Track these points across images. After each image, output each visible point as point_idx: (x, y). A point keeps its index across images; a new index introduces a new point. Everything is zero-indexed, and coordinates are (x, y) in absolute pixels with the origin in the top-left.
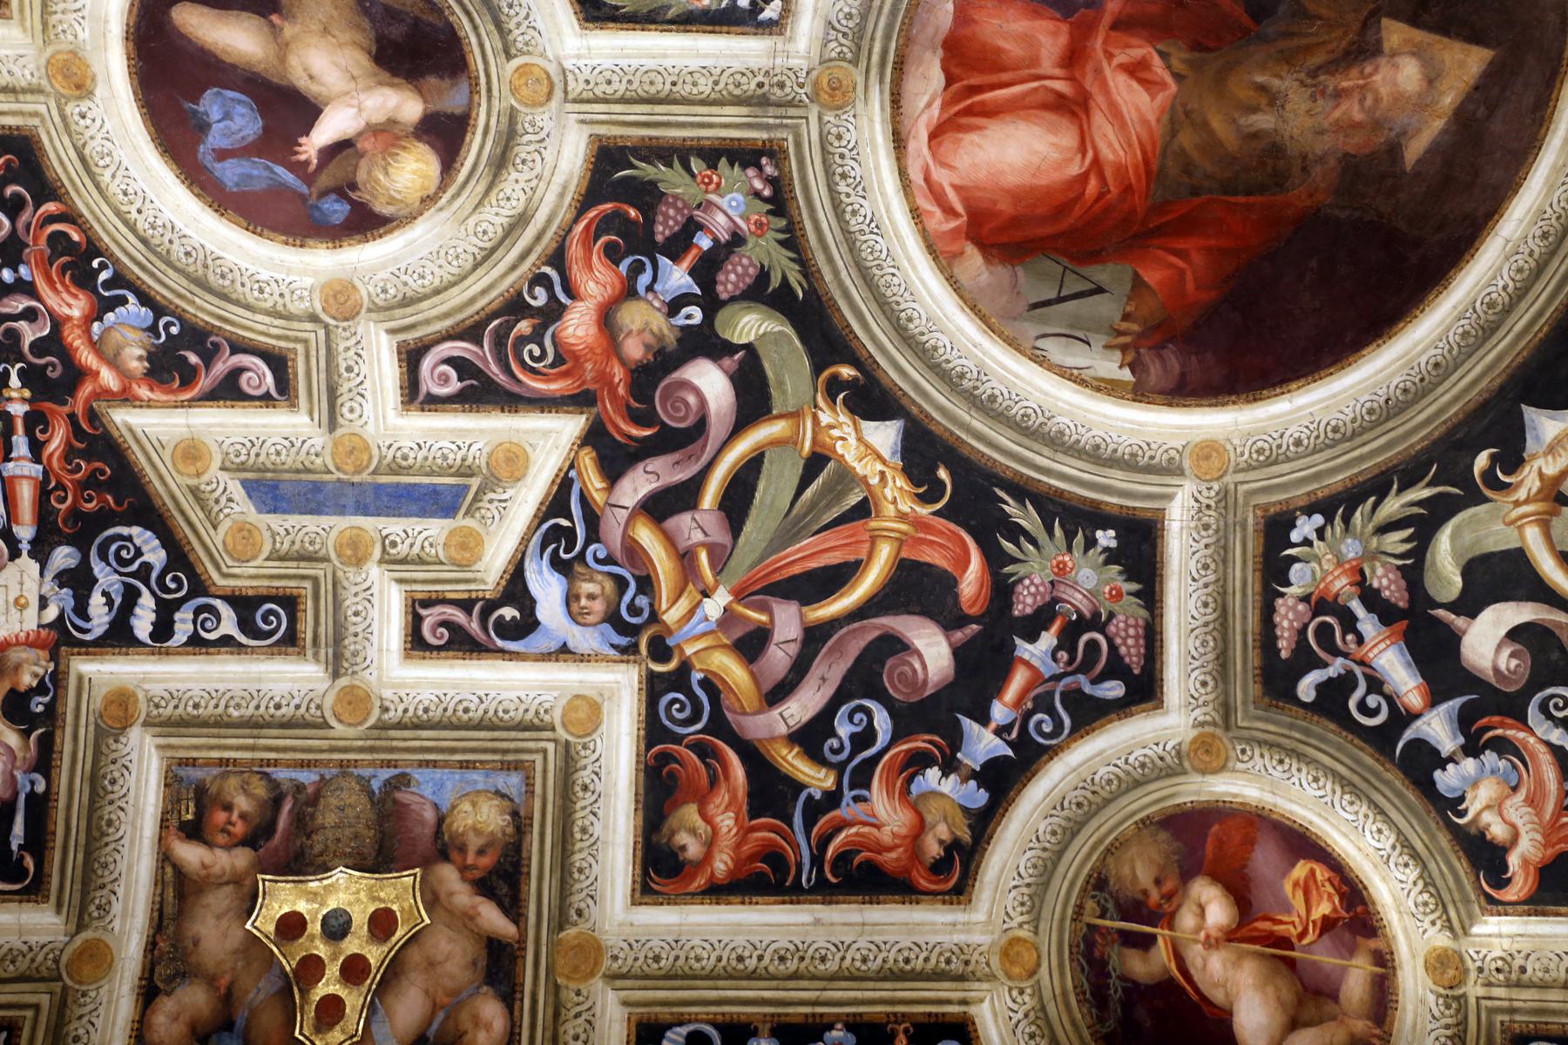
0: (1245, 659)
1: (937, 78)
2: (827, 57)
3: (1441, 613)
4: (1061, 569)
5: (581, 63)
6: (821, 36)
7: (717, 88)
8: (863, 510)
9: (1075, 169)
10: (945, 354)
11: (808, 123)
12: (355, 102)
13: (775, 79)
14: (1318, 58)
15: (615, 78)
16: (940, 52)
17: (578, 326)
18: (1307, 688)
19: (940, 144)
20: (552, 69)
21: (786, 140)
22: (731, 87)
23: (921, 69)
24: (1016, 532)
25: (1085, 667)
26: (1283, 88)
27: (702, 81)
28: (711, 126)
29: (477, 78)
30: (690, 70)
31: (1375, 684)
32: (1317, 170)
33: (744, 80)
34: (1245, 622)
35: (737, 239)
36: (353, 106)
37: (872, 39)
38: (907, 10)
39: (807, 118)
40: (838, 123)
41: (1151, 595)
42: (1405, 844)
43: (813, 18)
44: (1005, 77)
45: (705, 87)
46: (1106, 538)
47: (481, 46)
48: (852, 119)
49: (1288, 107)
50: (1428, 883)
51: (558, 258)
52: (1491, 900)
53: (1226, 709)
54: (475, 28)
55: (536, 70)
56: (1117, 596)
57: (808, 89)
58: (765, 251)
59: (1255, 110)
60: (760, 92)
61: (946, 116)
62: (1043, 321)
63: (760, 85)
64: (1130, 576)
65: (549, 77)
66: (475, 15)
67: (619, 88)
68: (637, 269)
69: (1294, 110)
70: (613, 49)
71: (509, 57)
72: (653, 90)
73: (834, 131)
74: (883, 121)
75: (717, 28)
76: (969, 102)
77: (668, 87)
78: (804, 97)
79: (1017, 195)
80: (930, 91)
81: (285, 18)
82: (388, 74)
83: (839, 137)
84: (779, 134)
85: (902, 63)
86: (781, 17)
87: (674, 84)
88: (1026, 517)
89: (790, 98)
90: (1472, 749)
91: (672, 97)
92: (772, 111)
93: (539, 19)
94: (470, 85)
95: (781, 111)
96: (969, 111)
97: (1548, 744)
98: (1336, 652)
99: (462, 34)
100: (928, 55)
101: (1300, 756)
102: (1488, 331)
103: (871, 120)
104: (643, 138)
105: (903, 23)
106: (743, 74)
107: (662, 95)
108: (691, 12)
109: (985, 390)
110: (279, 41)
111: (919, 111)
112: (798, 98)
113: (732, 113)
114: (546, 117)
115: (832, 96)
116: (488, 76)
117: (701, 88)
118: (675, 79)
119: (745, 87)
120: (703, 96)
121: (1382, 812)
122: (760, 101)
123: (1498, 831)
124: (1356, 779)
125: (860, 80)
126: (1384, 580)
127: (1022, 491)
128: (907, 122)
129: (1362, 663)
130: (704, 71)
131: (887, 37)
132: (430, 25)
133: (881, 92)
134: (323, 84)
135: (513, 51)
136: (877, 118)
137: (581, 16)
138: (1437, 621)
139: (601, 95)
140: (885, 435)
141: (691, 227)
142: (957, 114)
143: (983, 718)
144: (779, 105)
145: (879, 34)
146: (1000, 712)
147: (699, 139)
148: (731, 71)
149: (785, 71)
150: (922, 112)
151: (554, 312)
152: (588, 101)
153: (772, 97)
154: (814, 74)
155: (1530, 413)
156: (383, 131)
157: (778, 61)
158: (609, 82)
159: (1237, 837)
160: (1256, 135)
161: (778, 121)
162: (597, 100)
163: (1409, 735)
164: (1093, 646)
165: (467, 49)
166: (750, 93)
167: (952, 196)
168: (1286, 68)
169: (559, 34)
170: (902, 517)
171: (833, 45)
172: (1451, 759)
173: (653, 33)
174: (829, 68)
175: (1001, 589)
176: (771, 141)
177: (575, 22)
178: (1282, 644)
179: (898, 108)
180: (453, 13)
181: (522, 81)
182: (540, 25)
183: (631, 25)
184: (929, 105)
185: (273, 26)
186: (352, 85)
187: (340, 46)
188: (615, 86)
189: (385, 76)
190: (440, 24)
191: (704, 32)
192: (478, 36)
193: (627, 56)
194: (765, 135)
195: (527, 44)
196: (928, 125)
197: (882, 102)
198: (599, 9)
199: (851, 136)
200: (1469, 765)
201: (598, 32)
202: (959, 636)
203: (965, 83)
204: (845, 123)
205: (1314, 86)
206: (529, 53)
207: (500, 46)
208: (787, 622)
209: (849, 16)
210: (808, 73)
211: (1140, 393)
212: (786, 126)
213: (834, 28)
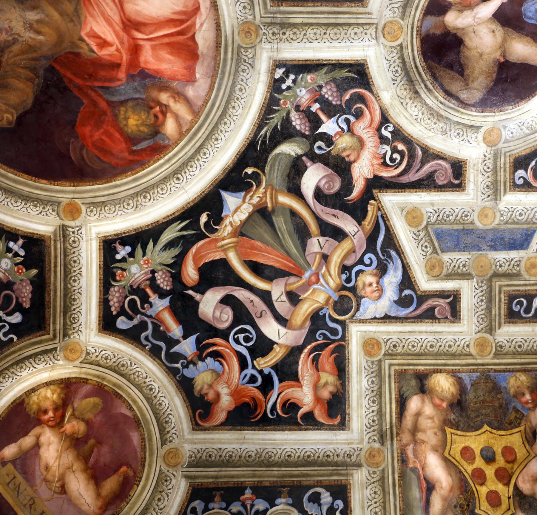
1: (200, 39)
2: (253, 49)
5: (368, 43)
6: (256, 61)
7: (305, 32)
11: (261, 15)
12: (476, 20)
13: (277, 37)
14: (16, 48)
15: (352, 36)
16: (199, 53)
19: (194, 5)
20: (382, 39)
21: (271, 6)
22: (298, 32)
23: (208, 43)
26: (28, 33)
27: (312, 35)
28: (308, 13)
29: (417, 34)
30: (317, 41)
33: (292, 36)
36: (478, 18)
37: (232, 59)
38: (217, 74)
39: (261, 17)
40: (246, 15)
43: (260, 69)
44: (166, 40)
45: (310, 32)
47: (413, 50)
48: (239, 17)
49: (22, 24)
54: (414, 59)
55: (389, 38)
57: (261, 32)
59: (38, 21)
60: (284, 30)
61: (193, 19)
63: (284, 34)
65: (384, 37)
66: (413, 66)
67: (351, 31)
69: (18, 21)
70: (352, 50)
71: (401, 45)
72: (335, 30)
73: (247, 11)
74: (224, 16)
75: (304, 63)
76: (182, 27)
77: (328, 32)
78: (263, 28)
80: (202, 32)
81: (498, 60)
82: (458, 34)
83: (245, 8)
84: (274, 9)
85: (217, 47)
86: (275, 70)
87: (325, 33)
89: (270, 28)
91: (326, 27)
92: (278, 21)
93: (385, 64)
94: (421, 31)
95: (274, 20)
96: (182, 22)
99: (421, 56)
100: (205, 51)
103: (229, 16)
104: (341, 6)
105: (218, 67)
106: (292, 39)
107: (331, 28)
108: (316, 71)
110: (503, 49)
111: (207, 21)
112: (266, 27)
113: (297, 19)
114: (388, 16)
115: (249, 28)
116: (412, 36)
117: (312, 32)
118: (325, 36)
119: (291, 32)
120: (311, 28)
122: (283, 25)
125: (236, 37)
128: (212, 16)
130: (310, 40)
131: (225, 60)
132: (434, 61)
133: (225, 31)
134: (489, 28)
135: (399, 48)
136: (226, 17)
137: (366, 66)
139: (360, 27)
142: (187, 20)
144: (275, 24)
145: (229, 62)
147: (314, 6)
148: (298, 41)
149: (272, 41)
150: (204, 21)
152: (366, 24)
153: (278, 27)
154: (258, 40)
156: (465, 7)
157: (276, 46)
158: (356, 34)
160: (34, 8)
161: (275, 16)
162: (362, 24)
165: (420, 49)
166: (289, 29)
168: (30, 43)
169: (377, 57)
171: (250, 56)
173: (334, 59)
174: (252, 43)
176: (278, 6)
177: (369, 63)
179: (216, 23)
180: (422, 67)
181: (396, 33)
182: (385, 62)
183: (344, 62)
184: (202, 25)
185: (504, 56)
186: (475, 28)
187: (477, 48)
188: (353, 32)
189: (459, 34)
190: (429, 61)
191: (310, 60)
192: (413, 55)
193: (346, 47)
194: (282, 8)
195: (392, 52)
196: (201, 14)
197: (225, 26)
198: (357, 70)
199: (239, 8)
201: (359, 59)
203: (186, 37)
204: (242, 15)
205: (12, 34)
206: (391, 47)
207: (404, 51)
209: (244, 71)
210: (261, 41)
212: (271, 13)
213: (250, 64)
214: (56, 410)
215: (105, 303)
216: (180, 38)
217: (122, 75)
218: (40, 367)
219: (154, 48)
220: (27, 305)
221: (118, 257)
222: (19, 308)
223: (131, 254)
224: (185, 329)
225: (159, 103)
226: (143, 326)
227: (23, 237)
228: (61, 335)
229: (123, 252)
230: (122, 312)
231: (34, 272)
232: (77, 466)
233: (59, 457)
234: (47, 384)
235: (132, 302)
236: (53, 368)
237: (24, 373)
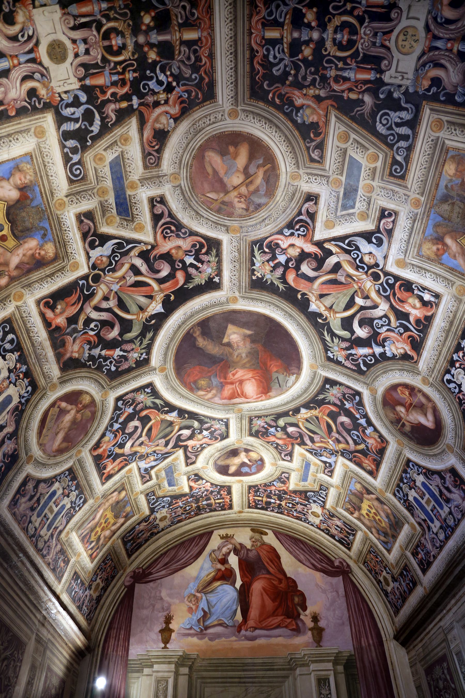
0: (356, 375)
3: (353, 338)
4: (333, 395)
8: (317, 418)
9: (254, 380)
10: (288, 400)
17: (280, 442)
18: (364, 369)
24: (324, 399)
25: (353, 400)
31: (366, 356)
32: (253, 346)
34: (349, 372)
35: (266, 422)
41: (341, 384)
42: (400, 370)
46: (327, 386)
50: (408, 371)
51: (268, 442)
52: (416, 362)
53: (365, 383)
56: (340, 389)
58: (268, 420)
62: (283, 385)
64: (336, 385)
68: (270, 434)
79: (258, 387)
88: (321, 397)
90: (384, 347)
97: (386, 331)
98: (357, 360)
101: (377, 377)
102: (291, 316)
109: (296, 396)
121: (392, 370)
123: (402, 351)
124: (384, 370)
126: (345, 345)
127: (317, 395)
129: (361, 356)
138: (354, 339)
140: (303, 411)
141: (263, 427)
143: (358, 419)
146: (358, 416)
151: (277, 444)
155: (310, 310)
159: (390, 396)
163: (378, 356)
164: (348, 396)
167: (259, 396)
170: (319, 413)
172: (385, 351)
175: (335, 405)
178: (354, 368)
200: (386, 348)
202: (342, 414)
208: (335, 435)
211: (299, 374)
214: (83, 406)
215: (127, 394)
216: (237, 395)
217: (222, 380)
218: (97, 389)
219: (233, 388)
220: (120, 370)
221: (146, 390)
222: (117, 367)
223: (148, 393)
224: (122, 422)
225: (211, 390)
226: (120, 409)
227: (148, 358)
228: (110, 387)
229: (148, 390)
230: (124, 401)
231: (134, 366)
232: (66, 430)
233: (67, 422)
234: (91, 396)
235: (129, 401)
236: (97, 393)
237: (93, 386)
